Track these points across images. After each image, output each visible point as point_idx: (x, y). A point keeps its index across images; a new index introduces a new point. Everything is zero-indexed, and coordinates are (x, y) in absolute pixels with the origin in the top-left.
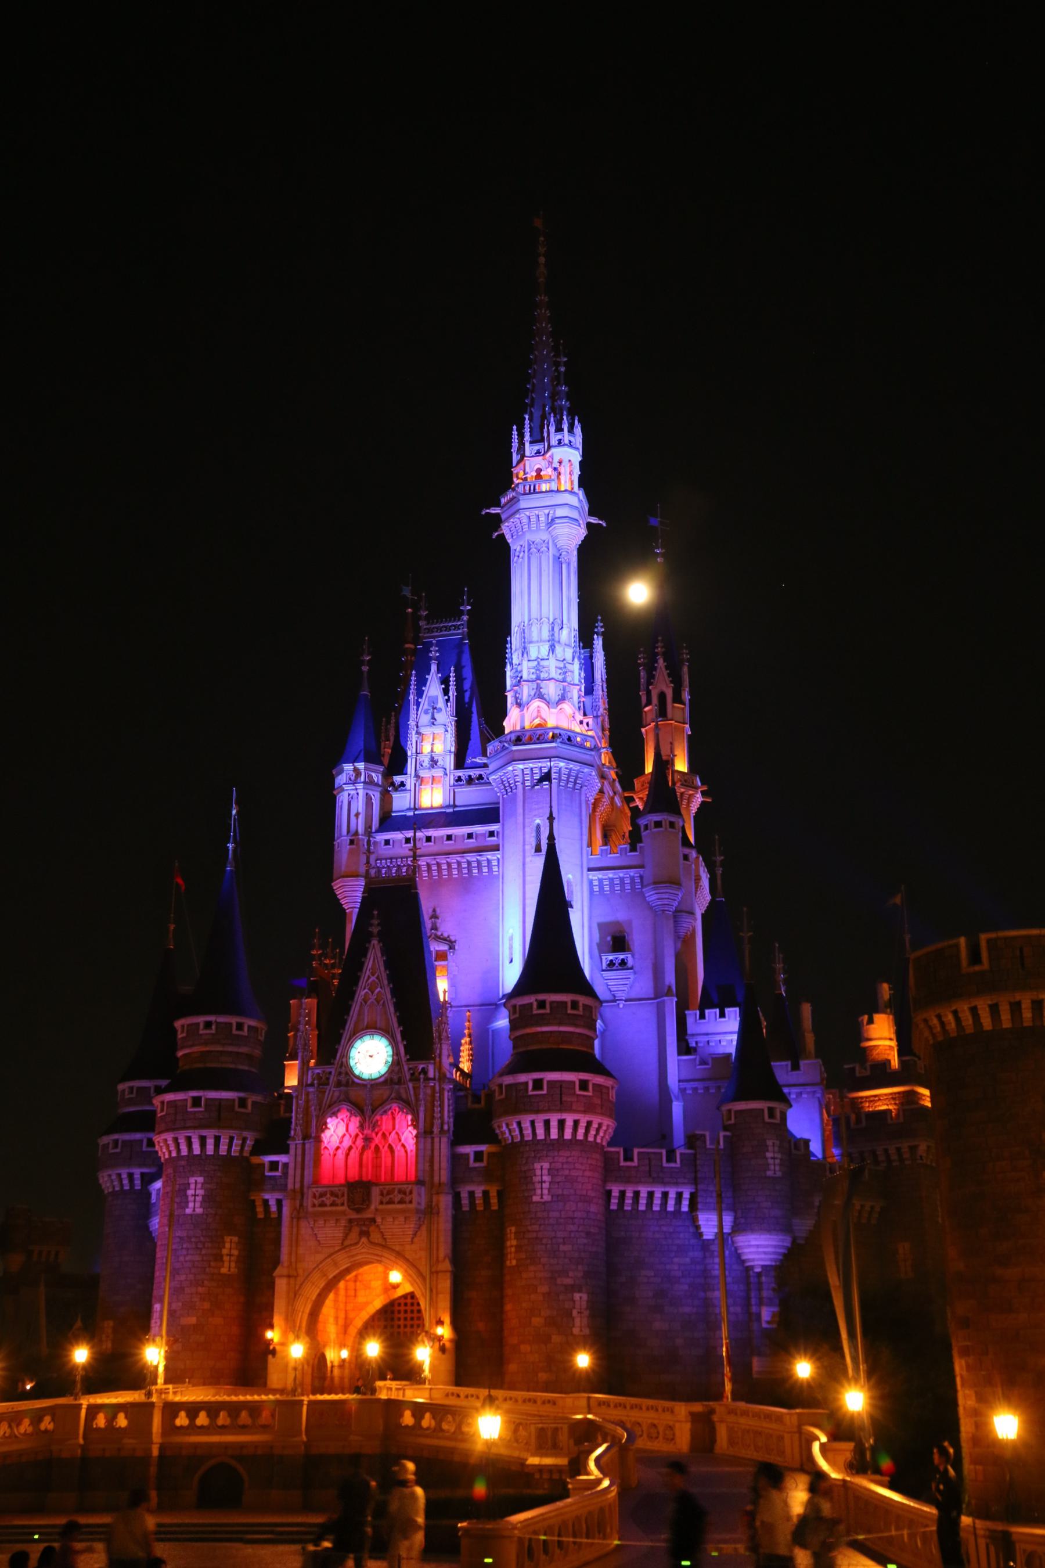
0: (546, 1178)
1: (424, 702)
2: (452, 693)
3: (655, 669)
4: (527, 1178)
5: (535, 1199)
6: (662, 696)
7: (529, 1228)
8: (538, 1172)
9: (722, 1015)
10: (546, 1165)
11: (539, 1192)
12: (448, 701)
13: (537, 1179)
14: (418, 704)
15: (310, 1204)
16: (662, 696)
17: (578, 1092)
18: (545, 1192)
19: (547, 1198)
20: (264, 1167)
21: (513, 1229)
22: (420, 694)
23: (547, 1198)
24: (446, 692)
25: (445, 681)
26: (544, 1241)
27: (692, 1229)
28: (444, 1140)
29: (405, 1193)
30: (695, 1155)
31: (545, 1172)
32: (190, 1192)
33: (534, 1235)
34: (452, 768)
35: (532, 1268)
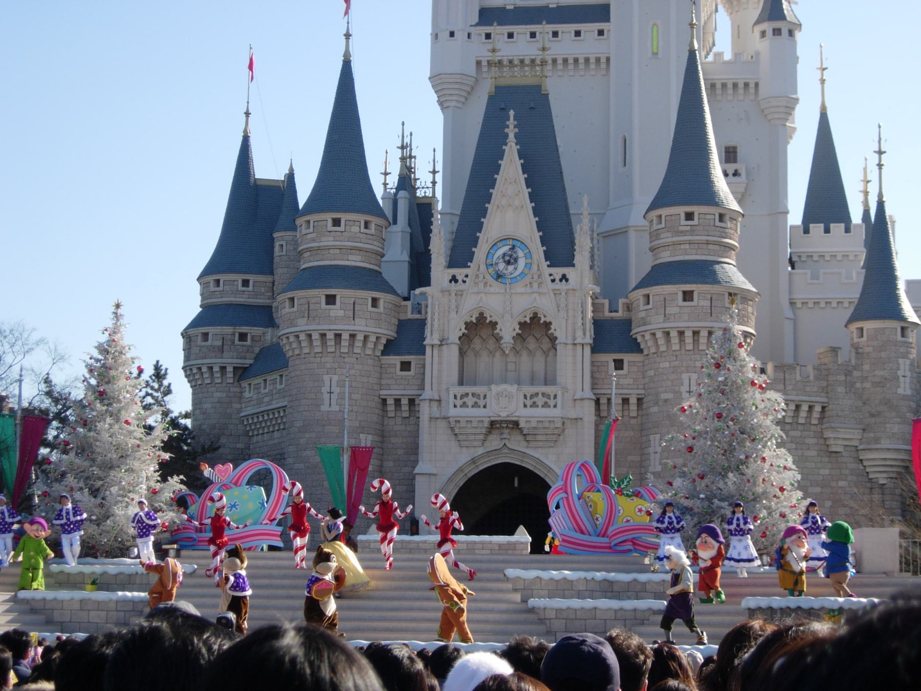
9: (827, 231)
15: (452, 406)
20: (395, 367)
28: (588, 350)
29: (549, 397)
32: (325, 390)
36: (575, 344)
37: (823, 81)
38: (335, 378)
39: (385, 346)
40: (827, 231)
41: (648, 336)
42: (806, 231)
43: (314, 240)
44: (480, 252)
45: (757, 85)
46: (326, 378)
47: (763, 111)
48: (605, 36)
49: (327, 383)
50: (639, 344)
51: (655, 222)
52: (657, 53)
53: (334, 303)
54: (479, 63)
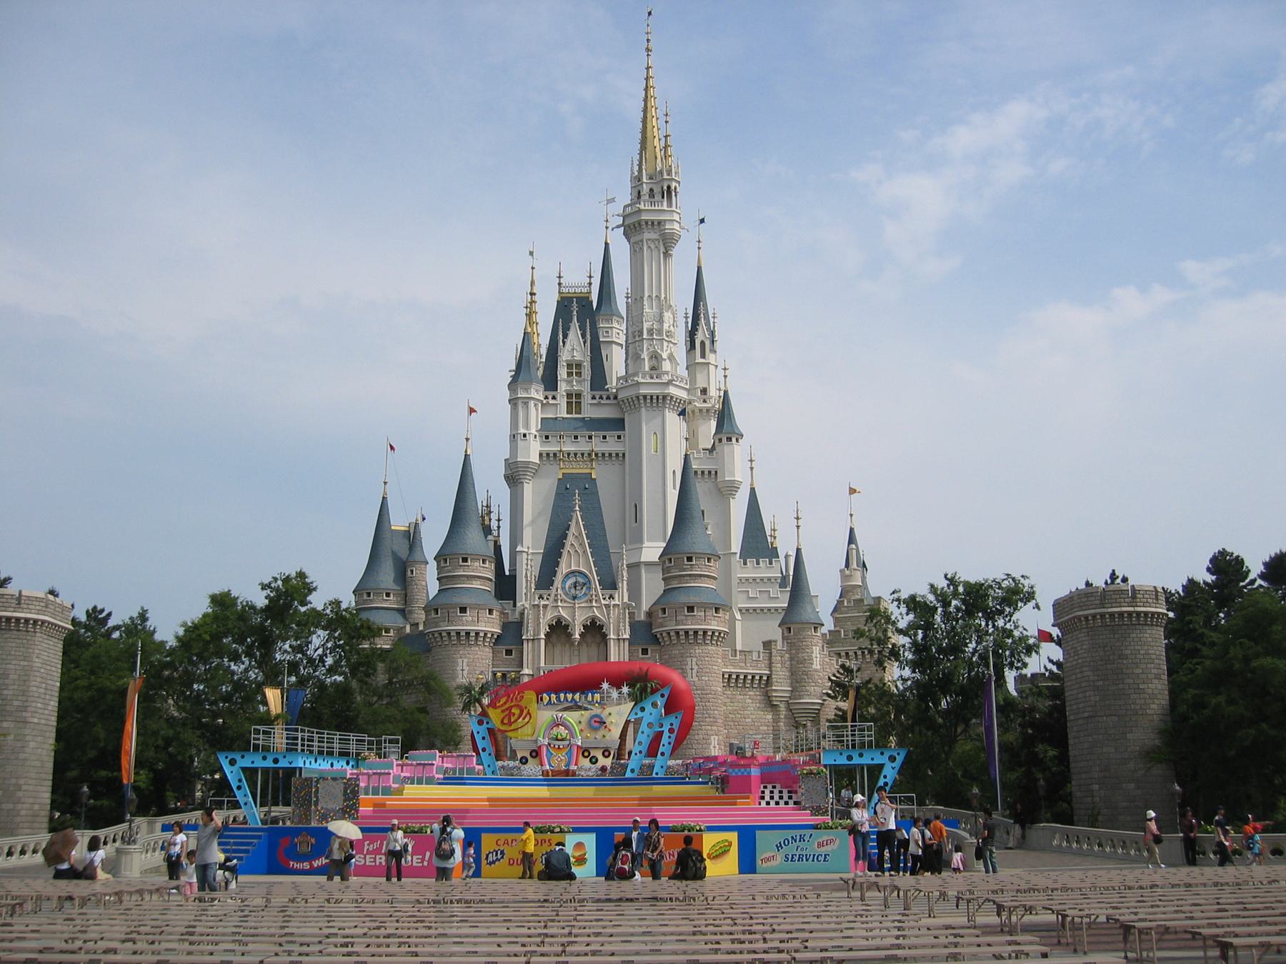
1: (568, 342)
2: (588, 336)
3: (698, 325)
6: (703, 343)
9: (758, 563)
12: (585, 343)
14: (564, 343)
16: (703, 343)
22: (565, 336)
24: (584, 336)
25: (582, 328)
27: (767, 698)
28: (627, 644)
30: (771, 653)
36: (619, 639)
37: (752, 468)
38: (466, 660)
39: (496, 640)
40: (758, 563)
41: (664, 634)
42: (745, 563)
43: (450, 571)
44: (558, 580)
46: (460, 660)
47: (719, 489)
48: (622, 439)
49: (461, 664)
50: (658, 639)
51: (667, 562)
53: (465, 612)
54: (541, 455)
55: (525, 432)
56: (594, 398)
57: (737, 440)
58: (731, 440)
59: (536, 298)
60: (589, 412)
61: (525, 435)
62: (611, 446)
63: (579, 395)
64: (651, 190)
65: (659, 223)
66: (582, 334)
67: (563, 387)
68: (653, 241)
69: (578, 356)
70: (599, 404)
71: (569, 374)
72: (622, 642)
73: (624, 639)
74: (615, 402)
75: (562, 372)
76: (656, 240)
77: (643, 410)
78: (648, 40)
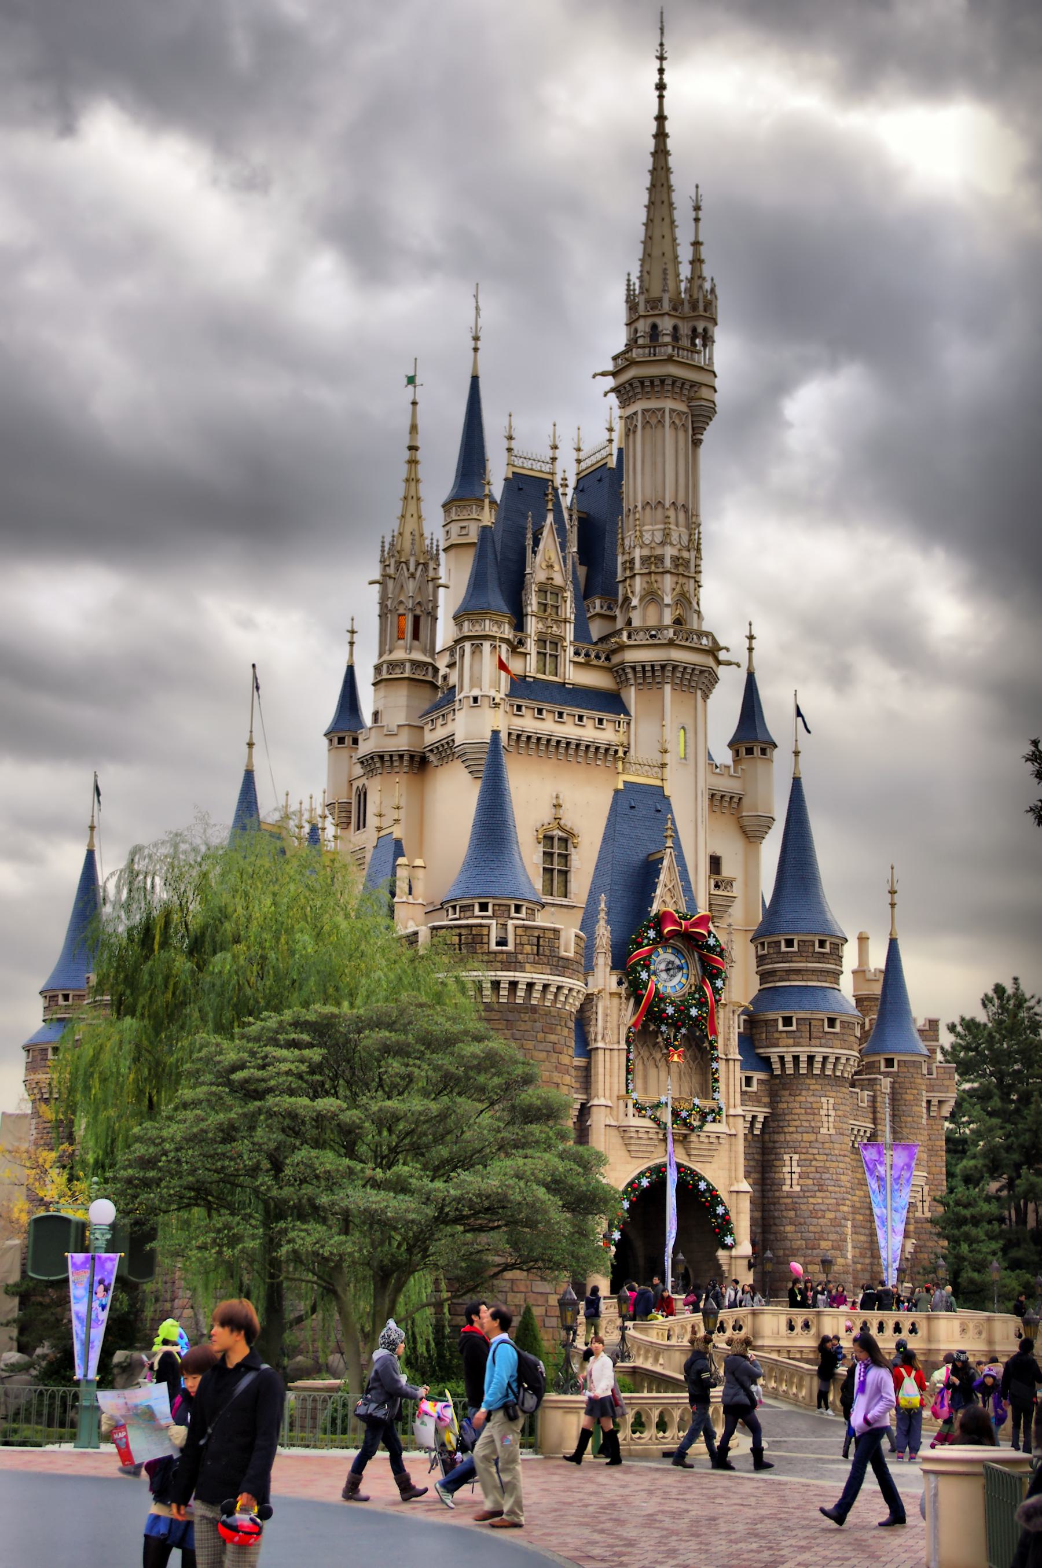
0: (832, 1113)
4: (813, 1111)
5: (823, 1131)
7: (817, 1157)
8: (825, 1106)
10: (832, 1101)
11: (825, 1125)
13: (823, 1112)
14: (534, 552)
17: (827, 1029)
18: (831, 1125)
19: (832, 1131)
21: (796, 1157)
22: (536, 542)
23: (832, 1131)
24: (563, 547)
26: (831, 1170)
31: (831, 1107)
33: (822, 1164)
34: (572, 639)
35: (818, 1194)
45: (740, 799)
52: (685, 758)
55: (476, 692)
56: (577, 653)
57: (763, 751)
58: (752, 754)
59: (420, 455)
60: (575, 676)
61: (475, 700)
62: (607, 735)
63: (557, 642)
64: (675, 328)
65: (694, 385)
66: (560, 543)
67: (533, 626)
68: (680, 413)
69: (558, 580)
70: (586, 665)
71: (544, 606)
72: (731, 1063)
73: (734, 1060)
74: (606, 664)
75: (533, 603)
76: (684, 413)
77: (668, 688)
78: (661, 71)
